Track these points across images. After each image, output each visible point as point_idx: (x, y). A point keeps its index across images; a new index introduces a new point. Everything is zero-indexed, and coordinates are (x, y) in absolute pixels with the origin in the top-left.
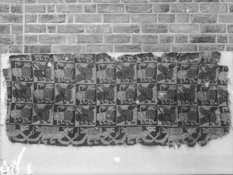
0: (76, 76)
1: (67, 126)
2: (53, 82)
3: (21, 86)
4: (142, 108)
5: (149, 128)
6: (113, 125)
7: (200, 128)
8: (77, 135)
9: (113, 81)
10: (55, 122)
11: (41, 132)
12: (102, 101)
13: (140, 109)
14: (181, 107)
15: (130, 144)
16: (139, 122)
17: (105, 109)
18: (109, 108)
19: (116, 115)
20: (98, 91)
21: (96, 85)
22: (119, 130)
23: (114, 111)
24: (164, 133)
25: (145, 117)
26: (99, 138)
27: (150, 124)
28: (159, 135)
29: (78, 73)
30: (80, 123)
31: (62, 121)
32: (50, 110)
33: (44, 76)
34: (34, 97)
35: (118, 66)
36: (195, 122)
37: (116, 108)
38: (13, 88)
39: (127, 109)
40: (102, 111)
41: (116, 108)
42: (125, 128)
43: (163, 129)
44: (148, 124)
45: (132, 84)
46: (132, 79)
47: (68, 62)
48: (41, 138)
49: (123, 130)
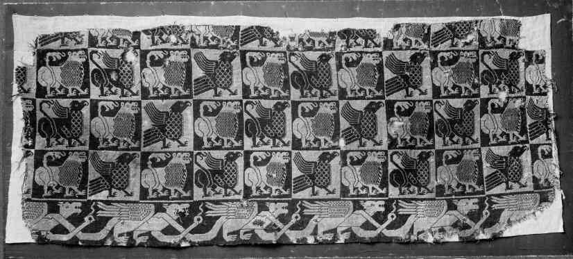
0: (193, 80)
1: (173, 199)
2: (138, 98)
3: (60, 109)
4: (351, 158)
5: (368, 203)
7: (485, 198)
8: (199, 220)
9: (283, 94)
10: (144, 193)
11: (111, 218)
12: (258, 140)
13: (348, 161)
14: (443, 151)
16: (345, 191)
17: (264, 158)
19: (289, 173)
20: (246, 117)
21: (241, 101)
24: (405, 213)
25: (360, 178)
26: (251, 226)
27: (372, 196)
29: (198, 72)
30: (205, 190)
31: (160, 188)
32: (131, 165)
33: (118, 84)
34: (91, 135)
35: (293, 59)
36: (473, 184)
37: (290, 156)
38: (39, 116)
40: (257, 164)
41: (291, 157)
42: (312, 205)
43: (402, 204)
45: (329, 102)
46: (327, 89)
47: (175, 47)
48: (111, 232)
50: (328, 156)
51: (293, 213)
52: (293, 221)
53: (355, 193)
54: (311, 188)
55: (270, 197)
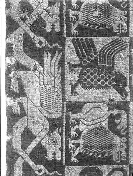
4: (119, 116)
6: (69, 28)
13: (116, 112)
15: (8, 81)
16: (75, 107)
18: (122, 12)
19: (99, 34)
22: (51, 44)
23: (112, 28)
25: (92, 127)
27: (67, 143)
28: (37, 172)
37: (123, 35)
39: (117, 70)
41: (120, 35)
44: (70, 136)
49: (51, 61)
50: (121, 85)
51: (46, 40)
52: (37, 39)
53: (71, 121)
54: (78, 62)
55: (67, 9)
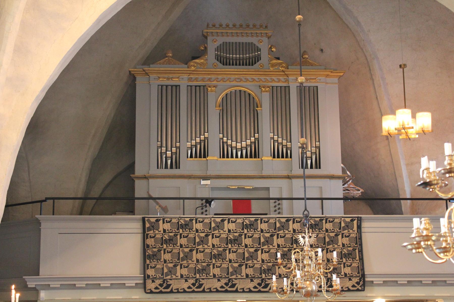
16: (247, 276)
